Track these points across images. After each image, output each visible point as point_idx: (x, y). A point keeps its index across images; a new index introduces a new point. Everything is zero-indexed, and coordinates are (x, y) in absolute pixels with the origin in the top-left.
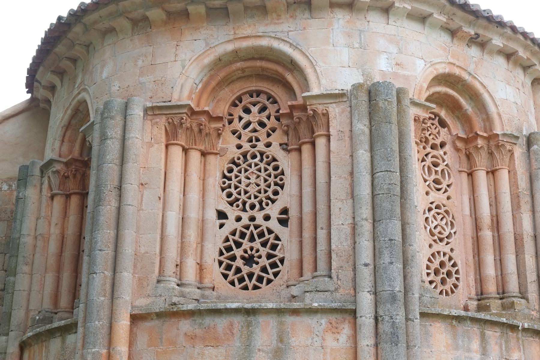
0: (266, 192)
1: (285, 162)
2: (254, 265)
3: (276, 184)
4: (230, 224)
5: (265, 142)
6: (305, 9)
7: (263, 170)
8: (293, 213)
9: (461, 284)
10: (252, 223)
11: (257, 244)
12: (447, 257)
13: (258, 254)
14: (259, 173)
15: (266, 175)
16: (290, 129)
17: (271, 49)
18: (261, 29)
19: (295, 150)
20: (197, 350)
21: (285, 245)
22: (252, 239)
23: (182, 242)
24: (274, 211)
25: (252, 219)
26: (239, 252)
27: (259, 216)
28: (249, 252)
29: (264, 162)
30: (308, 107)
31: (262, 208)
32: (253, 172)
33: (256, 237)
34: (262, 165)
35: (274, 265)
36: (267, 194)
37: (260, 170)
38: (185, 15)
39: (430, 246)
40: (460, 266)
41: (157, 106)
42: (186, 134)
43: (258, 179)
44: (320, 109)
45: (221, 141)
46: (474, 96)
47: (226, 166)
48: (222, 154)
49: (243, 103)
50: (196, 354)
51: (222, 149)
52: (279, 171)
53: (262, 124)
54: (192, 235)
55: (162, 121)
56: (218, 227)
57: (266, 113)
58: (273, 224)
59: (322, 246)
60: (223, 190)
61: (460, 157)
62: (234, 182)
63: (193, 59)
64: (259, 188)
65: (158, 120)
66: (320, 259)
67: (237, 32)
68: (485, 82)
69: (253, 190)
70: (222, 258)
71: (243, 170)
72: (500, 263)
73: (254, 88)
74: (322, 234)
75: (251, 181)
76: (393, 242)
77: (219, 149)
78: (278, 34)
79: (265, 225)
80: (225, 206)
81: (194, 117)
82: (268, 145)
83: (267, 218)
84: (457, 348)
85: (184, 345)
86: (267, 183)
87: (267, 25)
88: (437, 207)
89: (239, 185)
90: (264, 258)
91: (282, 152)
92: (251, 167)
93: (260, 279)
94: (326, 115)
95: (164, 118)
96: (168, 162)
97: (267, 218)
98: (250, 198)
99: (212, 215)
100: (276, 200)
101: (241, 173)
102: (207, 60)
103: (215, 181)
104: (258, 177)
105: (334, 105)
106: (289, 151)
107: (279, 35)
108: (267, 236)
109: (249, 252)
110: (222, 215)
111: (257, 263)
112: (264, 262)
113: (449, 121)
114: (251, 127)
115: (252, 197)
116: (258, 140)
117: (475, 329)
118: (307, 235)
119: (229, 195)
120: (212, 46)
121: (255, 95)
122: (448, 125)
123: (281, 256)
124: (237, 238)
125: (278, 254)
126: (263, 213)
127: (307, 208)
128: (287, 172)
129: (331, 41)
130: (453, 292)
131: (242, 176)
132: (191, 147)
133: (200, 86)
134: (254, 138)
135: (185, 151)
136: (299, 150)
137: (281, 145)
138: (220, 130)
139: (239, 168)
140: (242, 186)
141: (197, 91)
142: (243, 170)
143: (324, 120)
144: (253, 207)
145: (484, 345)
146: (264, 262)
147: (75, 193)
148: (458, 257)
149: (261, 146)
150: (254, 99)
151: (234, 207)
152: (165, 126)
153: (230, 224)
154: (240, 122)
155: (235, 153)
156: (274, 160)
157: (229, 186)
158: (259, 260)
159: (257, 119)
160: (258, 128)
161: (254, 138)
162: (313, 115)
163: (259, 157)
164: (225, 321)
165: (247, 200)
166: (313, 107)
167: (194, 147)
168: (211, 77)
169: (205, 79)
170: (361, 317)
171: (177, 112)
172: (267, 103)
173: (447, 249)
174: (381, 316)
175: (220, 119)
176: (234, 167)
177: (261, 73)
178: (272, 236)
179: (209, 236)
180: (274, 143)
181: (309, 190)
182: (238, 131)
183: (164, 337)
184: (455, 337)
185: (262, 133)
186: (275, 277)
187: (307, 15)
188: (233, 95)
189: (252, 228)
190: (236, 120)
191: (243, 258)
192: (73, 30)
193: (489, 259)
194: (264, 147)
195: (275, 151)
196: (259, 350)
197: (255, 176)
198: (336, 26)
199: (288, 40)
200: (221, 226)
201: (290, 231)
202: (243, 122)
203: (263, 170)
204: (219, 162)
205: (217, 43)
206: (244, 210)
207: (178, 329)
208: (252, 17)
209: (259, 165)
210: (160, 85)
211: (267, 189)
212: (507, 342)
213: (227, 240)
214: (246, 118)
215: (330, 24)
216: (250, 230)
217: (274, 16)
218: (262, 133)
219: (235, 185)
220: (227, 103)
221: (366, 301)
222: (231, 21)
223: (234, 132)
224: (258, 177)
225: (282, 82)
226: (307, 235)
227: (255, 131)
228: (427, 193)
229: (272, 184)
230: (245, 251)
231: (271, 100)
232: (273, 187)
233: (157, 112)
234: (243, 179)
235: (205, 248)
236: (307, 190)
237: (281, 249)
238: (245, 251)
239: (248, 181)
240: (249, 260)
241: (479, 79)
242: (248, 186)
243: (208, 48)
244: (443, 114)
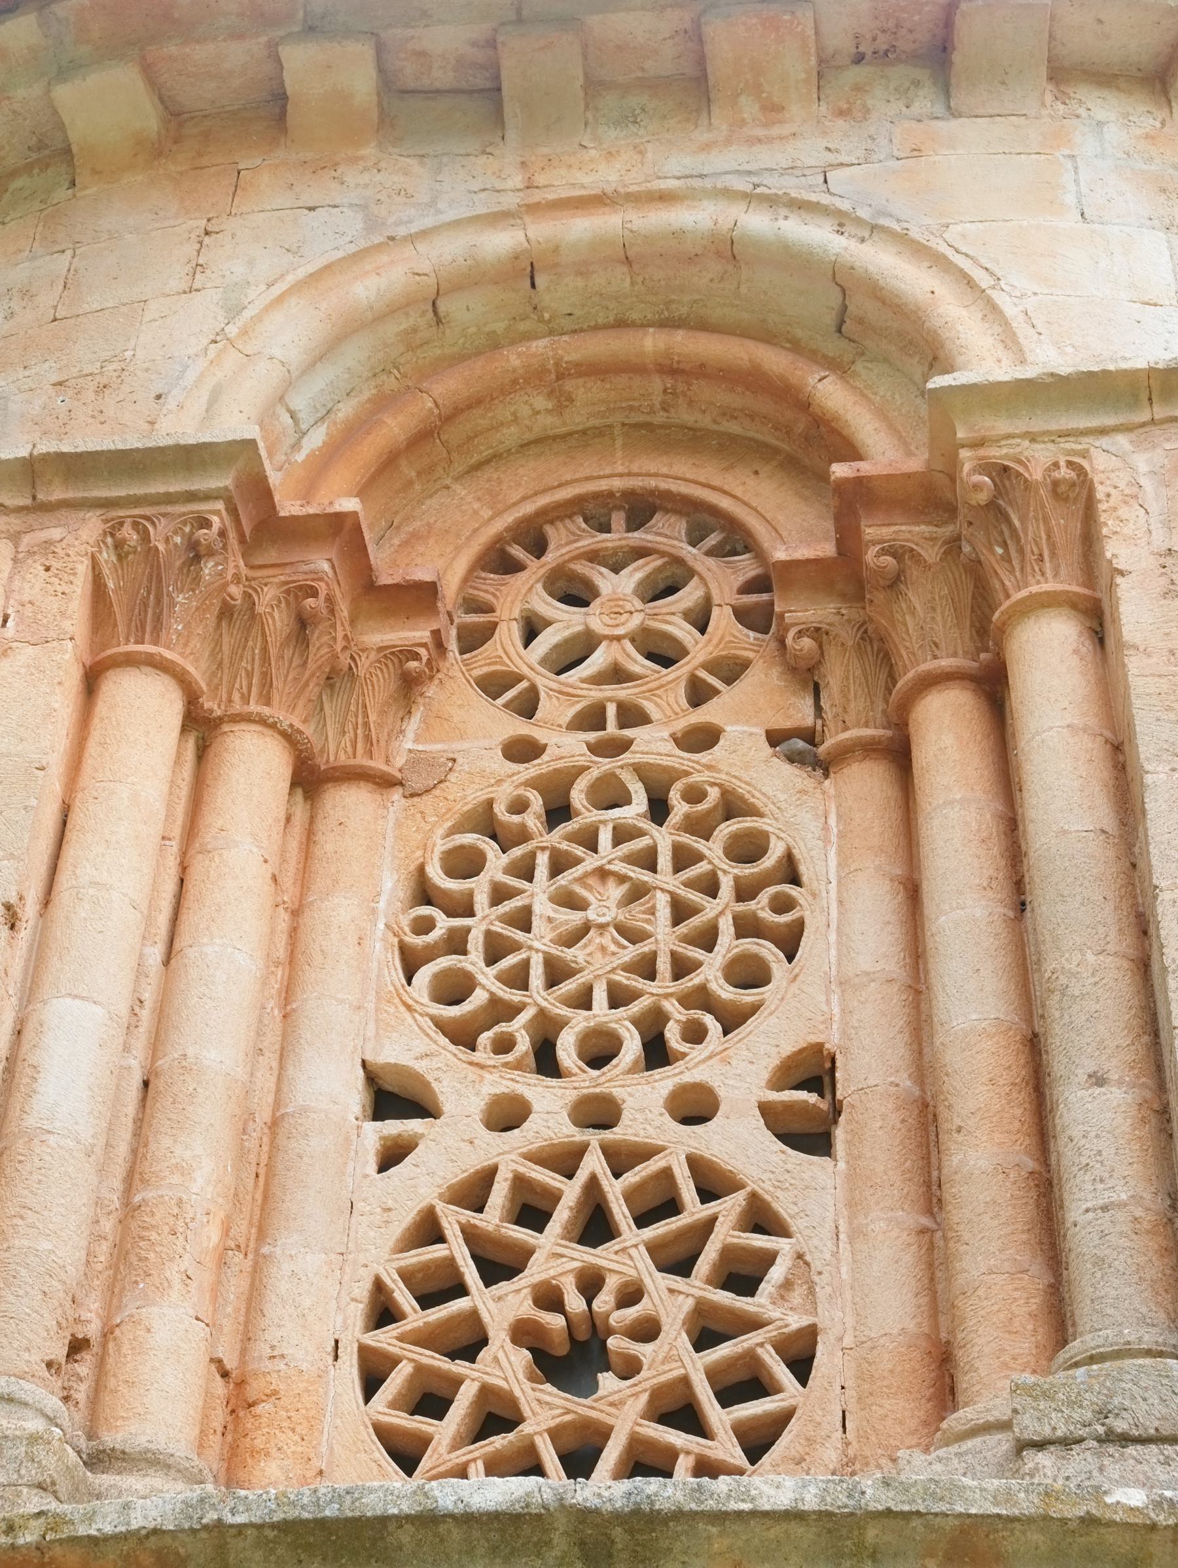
0: (682, 967)
1: (804, 816)
2: (607, 1381)
3: (747, 927)
4: (451, 1146)
5: (680, 725)
6: (917, 83)
7: (664, 860)
8: (871, 1076)
10: (594, 1138)
11: (629, 1254)
13: (632, 1313)
14: (645, 876)
15: (688, 884)
16: (832, 652)
17: (729, 250)
18: (673, 162)
19: (868, 749)
21: (820, 1253)
22: (595, 1226)
23: (130, 1209)
24: (740, 1070)
25: (599, 1113)
26: (500, 1306)
27: (643, 1103)
28: (575, 1302)
29: (675, 817)
30: (964, 454)
31: (656, 1053)
32: (602, 874)
33: (621, 1213)
34: (663, 839)
35: (741, 1385)
36: (692, 981)
37: (648, 861)
38: (270, 114)
41: (61, 456)
42: (218, 643)
43: (637, 907)
44: (1038, 460)
45: (413, 724)
47: (441, 845)
48: (416, 783)
49: (551, 558)
51: (416, 760)
52: (768, 862)
53: (663, 654)
54: (198, 1167)
55: (80, 539)
56: (372, 1167)
57: (689, 596)
58: (740, 1141)
62: (485, 920)
63: (290, 279)
64: (645, 947)
65: (56, 533)
66: (1099, 1262)
67: (540, 179)
69: (602, 961)
70: (385, 1339)
71: (543, 860)
73: (617, 484)
75: (591, 914)
77: (399, 761)
78: (767, 179)
79: (679, 1146)
80: (421, 1045)
81: (272, 555)
82: (702, 739)
83: (694, 1108)
86: (695, 921)
87: (706, 147)
89: (519, 936)
90: (675, 1337)
91: (789, 771)
92: (592, 846)
94: (1078, 495)
95: (91, 526)
96: (92, 748)
97: (694, 1108)
98: (584, 1001)
99: (332, 1091)
100: (754, 1009)
101: (530, 879)
102: (367, 288)
103: (364, 908)
104: (638, 893)
105: (1122, 441)
106: (824, 767)
107: (775, 184)
108: (694, 1210)
109: (575, 1302)
110: (394, 1098)
111: (630, 1369)
112: (673, 1358)
114: (598, 661)
115: (600, 996)
116: (632, 716)
119: (453, 989)
120: (402, 231)
121: (618, 520)
123: (796, 1322)
124: (493, 1217)
125: (774, 1313)
126: (665, 1081)
127: (972, 1000)
129: (1070, 199)
131: (538, 894)
132: (237, 707)
133: (316, 439)
134: (611, 710)
135: (201, 727)
136: (899, 755)
137: (775, 738)
138: (416, 657)
139: (517, 852)
140: (539, 943)
141: (300, 457)
142: (543, 860)
143: (1064, 524)
144: (600, 1053)
146: (673, 1358)
149: (653, 744)
150: (617, 538)
151: (480, 1056)
152: (95, 564)
153: (451, 1146)
154: (526, 645)
155: (494, 780)
156: (732, 807)
157: (456, 943)
158: (644, 1351)
159: (636, 621)
160: (639, 664)
161: (611, 710)
162: (992, 506)
163: (640, 803)
165: (564, 1011)
166: (995, 453)
167: (254, 707)
168: (382, 403)
169: (346, 410)
172: (688, 552)
175: (420, 597)
176: (490, 847)
177: (659, 418)
178: (729, 1208)
179: (309, 1207)
180: (732, 731)
181: (978, 913)
182: (519, 678)
185: (664, 696)
186: (753, 1460)
187: (925, 101)
188: (498, 514)
189: (594, 1163)
190: (509, 633)
191: (524, 1333)
194: (671, 747)
195: (744, 760)
197: (616, 892)
199: (825, 199)
200: (392, 1156)
201: (853, 1177)
202: (545, 641)
203: (664, 860)
204: (398, 825)
205: (428, 222)
206: (545, 1061)
208: (630, 119)
209: (641, 833)
211: (696, 953)
213: (428, 1230)
214: (566, 622)
216: (582, 1176)
217: (749, 107)
218: (664, 696)
219: (489, 935)
220: (458, 549)
222: (511, 134)
223: (493, 685)
224: (638, 893)
225: (776, 451)
227: (617, 675)
229: (726, 927)
230: (549, 1298)
231: (713, 540)
232: (728, 943)
233: (58, 493)
234: (542, 907)
235: (280, 1283)
236: (964, 908)
237: (787, 1285)
238: (549, 1298)
239: (576, 918)
242: (573, 938)
243: (378, 239)
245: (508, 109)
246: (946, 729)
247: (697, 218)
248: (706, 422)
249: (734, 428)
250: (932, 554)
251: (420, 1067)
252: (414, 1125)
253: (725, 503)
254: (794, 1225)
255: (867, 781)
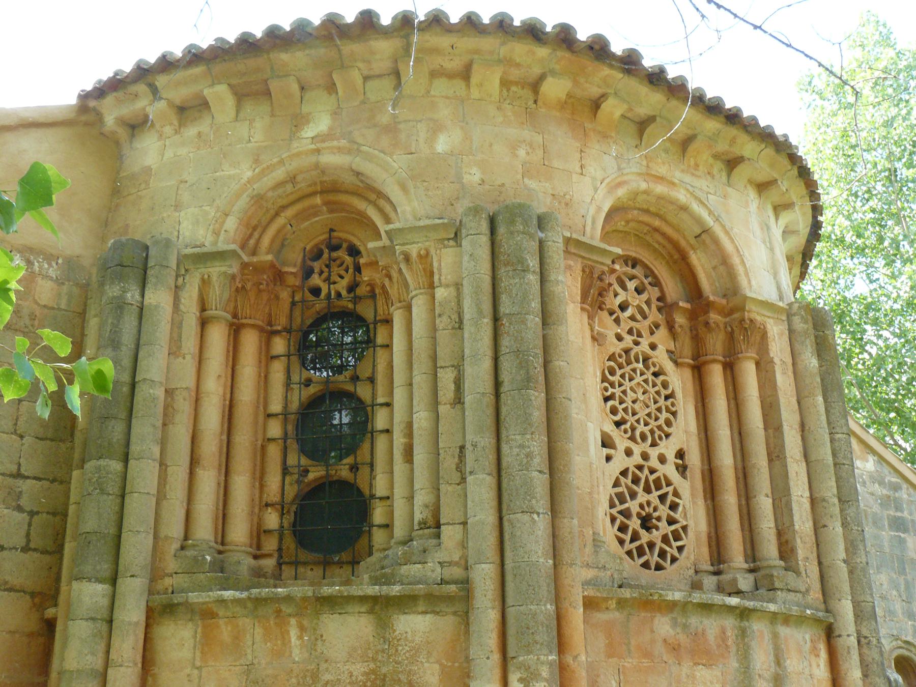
0: (657, 419)
20: (685, 669)
21: (687, 507)
50: (684, 675)
58: (669, 470)
59: (767, 525)
60: (606, 399)
74: (764, 504)
85: (665, 658)
93: (663, 554)
97: (662, 459)
118: (730, 499)
123: (685, 523)
125: (681, 520)
128: (679, 394)
137: (668, 351)
147: (253, 326)
153: (620, 461)
158: (659, 524)
164: (715, 624)
170: (848, 636)
171: (600, 260)
174: (866, 637)
183: (633, 642)
192: (373, 43)
196: (759, 675)
200: (608, 458)
207: (652, 631)
210: (563, 204)
221: (484, 576)
226: (730, 499)
238: (641, 506)
240: (647, 523)
245: (645, 136)
246: (716, 376)
247: (682, 196)
248: (651, 241)
249: (657, 246)
250: (722, 326)
251: (611, 433)
252: (612, 452)
253: (656, 272)
254: (683, 497)
255: (688, 373)
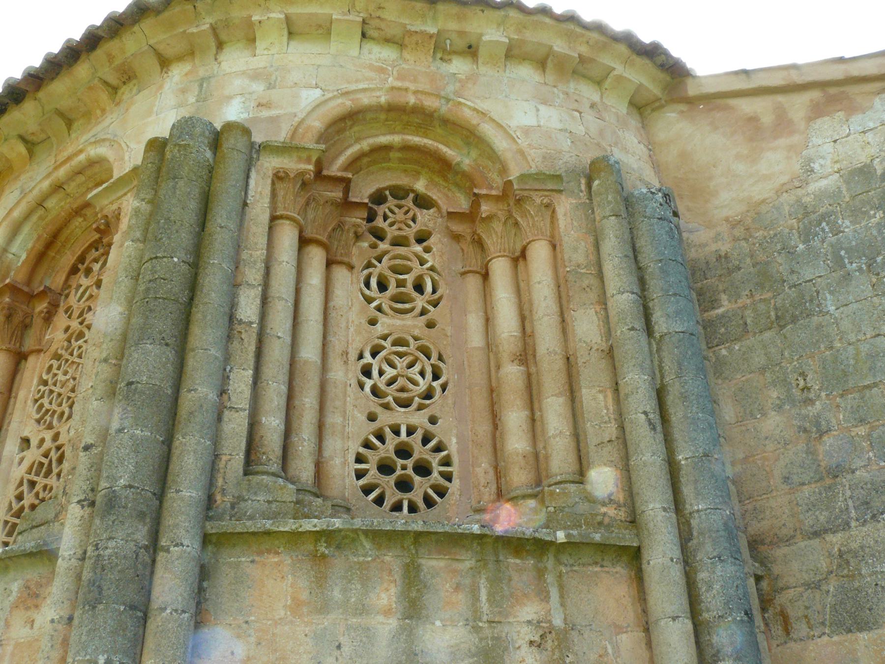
9: (454, 487)
12: (418, 435)
39: (372, 418)
40: (453, 447)
46: (470, 137)
61: (463, 250)
68: (482, 105)
72: (534, 423)
76: (133, 387)
84: (324, 608)
88: (397, 342)
113: (434, 195)
117: (387, 558)
122: (436, 202)
130: (429, 503)
145: (414, 594)
148: (449, 433)
173: (420, 419)
184: (320, 581)
193: (515, 418)
198: (167, 86)
205: (33, 184)
212: (495, 582)
215: (161, 87)
228: (373, 322)
241: (469, 103)
244: (420, 186)
